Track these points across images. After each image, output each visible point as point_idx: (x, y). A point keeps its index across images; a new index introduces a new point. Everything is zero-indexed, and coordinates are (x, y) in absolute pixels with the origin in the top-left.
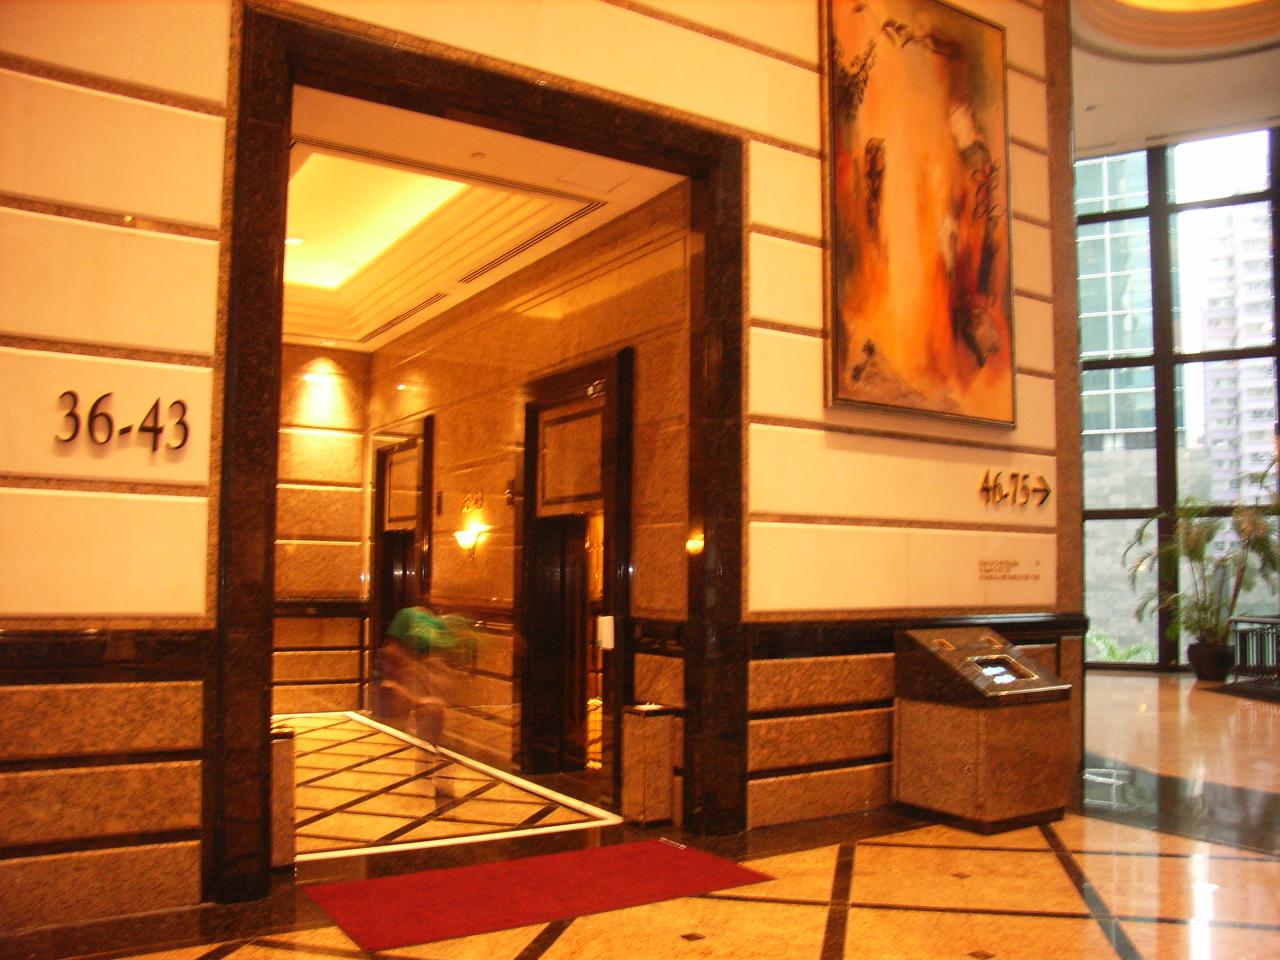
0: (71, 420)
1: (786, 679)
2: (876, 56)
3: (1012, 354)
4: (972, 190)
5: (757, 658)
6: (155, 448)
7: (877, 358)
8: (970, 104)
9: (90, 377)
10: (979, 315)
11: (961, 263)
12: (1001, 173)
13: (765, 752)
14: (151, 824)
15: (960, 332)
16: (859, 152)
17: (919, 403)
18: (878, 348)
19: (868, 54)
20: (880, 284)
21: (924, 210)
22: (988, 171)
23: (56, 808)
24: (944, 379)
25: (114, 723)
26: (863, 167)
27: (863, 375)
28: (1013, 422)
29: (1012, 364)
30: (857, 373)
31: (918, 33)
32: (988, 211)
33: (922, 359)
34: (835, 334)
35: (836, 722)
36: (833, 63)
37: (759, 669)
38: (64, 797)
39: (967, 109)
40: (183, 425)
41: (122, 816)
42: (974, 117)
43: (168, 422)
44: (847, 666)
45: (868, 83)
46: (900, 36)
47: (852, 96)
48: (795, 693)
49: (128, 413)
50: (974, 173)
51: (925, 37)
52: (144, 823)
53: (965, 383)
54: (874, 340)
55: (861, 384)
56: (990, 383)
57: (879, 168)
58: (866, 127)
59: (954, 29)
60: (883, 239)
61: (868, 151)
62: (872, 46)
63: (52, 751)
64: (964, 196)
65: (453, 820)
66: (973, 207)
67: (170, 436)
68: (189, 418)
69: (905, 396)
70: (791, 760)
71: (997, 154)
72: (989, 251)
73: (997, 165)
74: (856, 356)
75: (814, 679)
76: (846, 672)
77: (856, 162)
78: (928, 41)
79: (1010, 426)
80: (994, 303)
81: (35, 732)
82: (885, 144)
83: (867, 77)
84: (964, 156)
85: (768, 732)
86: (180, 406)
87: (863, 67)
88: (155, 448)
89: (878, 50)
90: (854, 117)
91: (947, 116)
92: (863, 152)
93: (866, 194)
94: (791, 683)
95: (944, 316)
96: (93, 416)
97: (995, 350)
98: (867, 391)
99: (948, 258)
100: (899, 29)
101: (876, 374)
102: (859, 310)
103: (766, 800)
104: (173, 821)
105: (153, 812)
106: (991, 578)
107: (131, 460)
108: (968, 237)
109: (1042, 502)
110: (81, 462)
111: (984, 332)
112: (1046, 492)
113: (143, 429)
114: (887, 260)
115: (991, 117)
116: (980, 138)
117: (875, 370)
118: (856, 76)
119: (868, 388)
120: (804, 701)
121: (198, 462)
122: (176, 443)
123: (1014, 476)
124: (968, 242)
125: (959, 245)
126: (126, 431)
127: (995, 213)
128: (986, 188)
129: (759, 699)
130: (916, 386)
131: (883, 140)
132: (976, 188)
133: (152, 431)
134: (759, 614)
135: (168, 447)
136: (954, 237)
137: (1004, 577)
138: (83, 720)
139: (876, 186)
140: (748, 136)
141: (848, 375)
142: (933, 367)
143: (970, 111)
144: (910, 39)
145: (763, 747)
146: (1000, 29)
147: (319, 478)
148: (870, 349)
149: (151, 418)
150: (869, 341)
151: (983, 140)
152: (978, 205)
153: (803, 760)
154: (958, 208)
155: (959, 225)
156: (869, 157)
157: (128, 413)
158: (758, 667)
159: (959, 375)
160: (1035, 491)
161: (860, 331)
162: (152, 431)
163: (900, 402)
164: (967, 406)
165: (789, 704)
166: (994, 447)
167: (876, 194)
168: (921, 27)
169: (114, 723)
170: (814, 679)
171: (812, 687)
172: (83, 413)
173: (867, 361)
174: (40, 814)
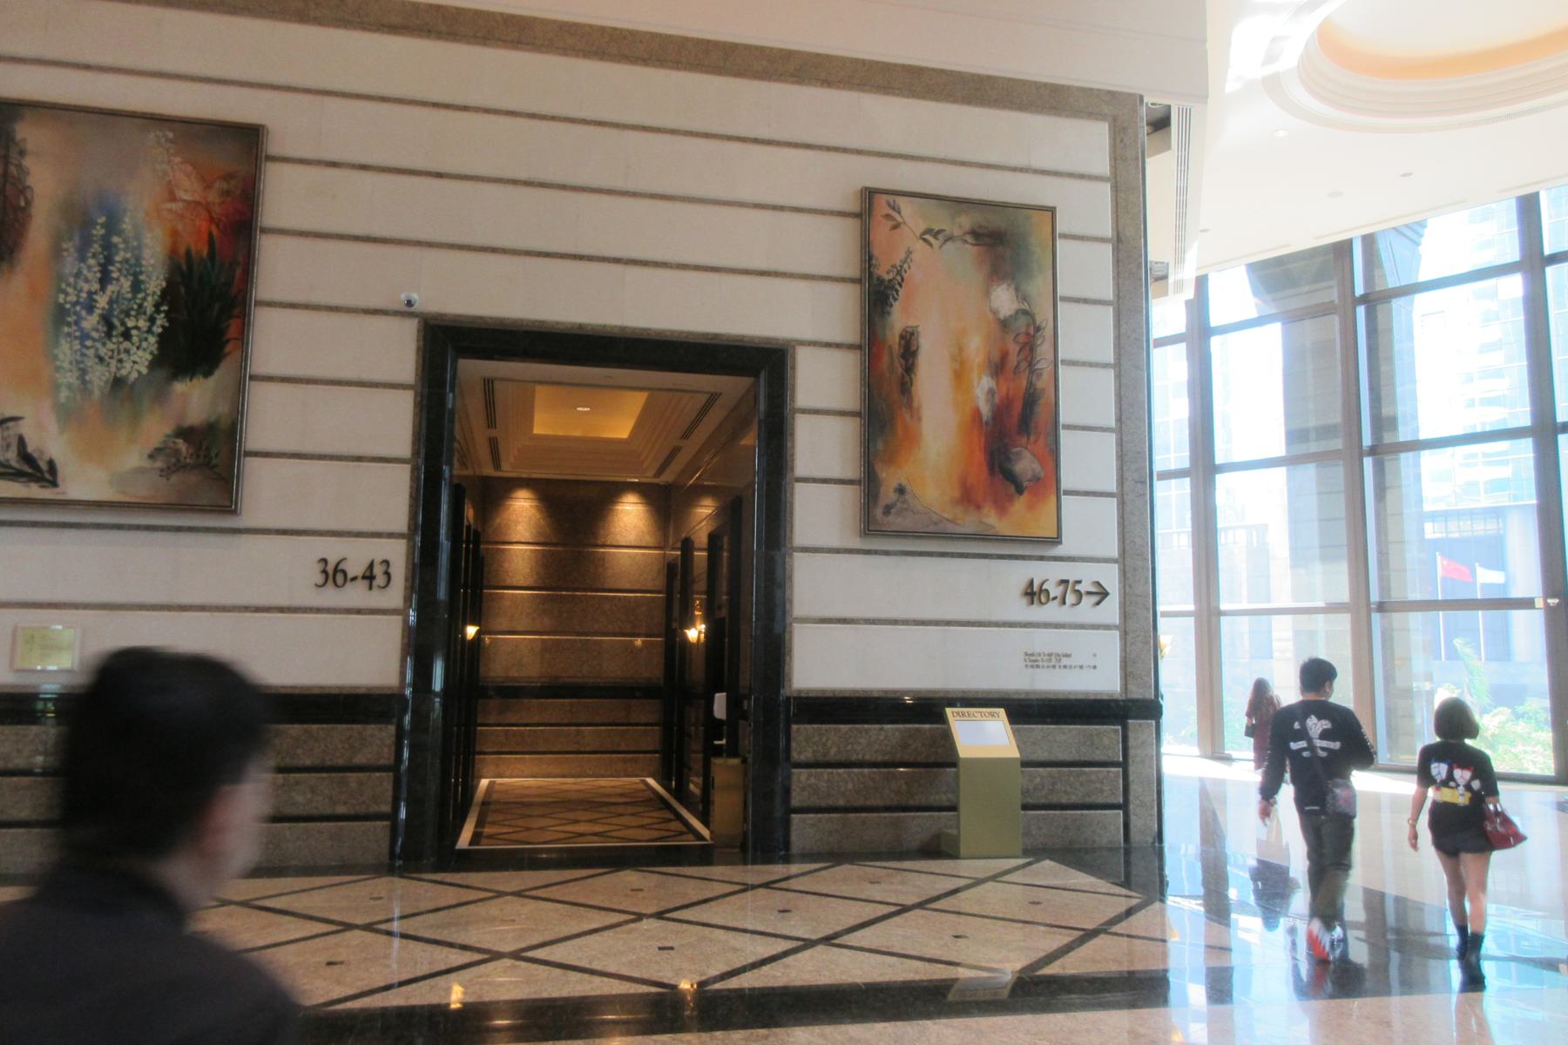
0: (324, 575)
1: (824, 739)
2: (911, 260)
3: (1058, 481)
4: (1013, 349)
5: (797, 722)
6: (371, 588)
7: (907, 497)
8: (1013, 279)
9: (334, 550)
10: (1018, 453)
11: (1001, 411)
12: (1048, 332)
13: (806, 793)
14: (362, 810)
15: (997, 469)
16: (893, 336)
17: (950, 528)
18: (908, 488)
19: (905, 261)
20: (912, 438)
21: (960, 375)
22: (1032, 332)
23: (309, 796)
24: (978, 507)
25: (343, 748)
26: (896, 350)
27: (893, 511)
28: (1057, 538)
29: (1058, 489)
30: (888, 510)
31: (957, 232)
32: (1031, 365)
33: (956, 493)
34: (869, 483)
35: (872, 776)
36: (870, 273)
37: (801, 731)
38: (313, 790)
39: (1009, 285)
40: (387, 574)
41: (345, 803)
42: (1017, 290)
43: (378, 570)
44: (883, 733)
45: (903, 284)
46: (937, 239)
47: (887, 298)
48: (833, 751)
49: (355, 568)
50: (1015, 337)
51: (965, 234)
52: (357, 808)
53: (1002, 507)
54: (904, 482)
55: (891, 518)
56: (1031, 507)
57: (913, 348)
58: (897, 320)
59: (996, 221)
60: (915, 405)
61: (902, 337)
62: (909, 252)
63: (308, 762)
64: (1004, 356)
65: (555, 818)
66: (1015, 363)
67: (380, 580)
68: (392, 570)
69: (936, 524)
70: (830, 802)
71: (1043, 315)
72: (1031, 399)
73: (1043, 325)
74: (888, 494)
75: (850, 741)
76: (882, 738)
77: (890, 346)
78: (969, 238)
79: (1056, 540)
80: (1036, 441)
81: (299, 751)
82: (920, 329)
83: (903, 279)
84: (1004, 324)
85: (808, 779)
86: (386, 562)
87: (899, 273)
88: (371, 588)
89: (916, 256)
90: (889, 313)
91: (987, 293)
92: (897, 339)
93: (900, 370)
94: (829, 744)
95: (980, 457)
96: (336, 570)
97: (1037, 479)
98: (896, 522)
99: (985, 410)
100: (936, 234)
101: (906, 509)
102: (891, 459)
103: (803, 830)
104: (374, 809)
105: (364, 802)
106: (1038, 666)
107: (355, 595)
108: (1008, 390)
109: (1098, 603)
110: (331, 597)
111: (1025, 465)
112: (1103, 594)
113: (364, 577)
114: (920, 419)
115: (1038, 286)
116: (1025, 306)
117: (905, 506)
118: (890, 281)
119: (899, 520)
120: (842, 758)
121: (395, 595)
122: (382, 584)
123: (1064, 582)
124: (1008, 395)
125: (997, 399)
126: (354, 579)
127: (1039, 366)
128: (1029, 346)
129: (799, 753)
130: (946, 515)
131: (917, 327)
132: (1017, 348)
133: (369, 577)
134: (800, 691)
135: (379, 587)
136: (991, 392)
137: (1054, 667)
138: (326, 746)
139: (909, 364)
140: (793, 343)
141: (878, 512)
142: (967, 498)
143: (1013, 286)
144: (950, 238)
145: (803, 789)
146: (1052, 210)
147: (627, 586)
148: (901, 490)
149: (369, 571)
150: (900, 485)
151: (1027, 308)
152: (1019, 363)
153: (841, 802)
154: (998, 368)
155: (997, 384)
156: (903, 342)
157: (355, 568)
158: (799, 729)
159: (995, 502)
160: (1089, 593)
161: (890, 478)
162: (369, 577)
163: (932, 528)
164: (1003, 527)
165: (827, 759)
166: (1041, 558)
167: (909, 369)
168: (960, 227)
169: (343, 748)
170: (850, 741)
171: (849, 747)
172: (330, 569)
173: (898, 500)
174: (300, 799)
